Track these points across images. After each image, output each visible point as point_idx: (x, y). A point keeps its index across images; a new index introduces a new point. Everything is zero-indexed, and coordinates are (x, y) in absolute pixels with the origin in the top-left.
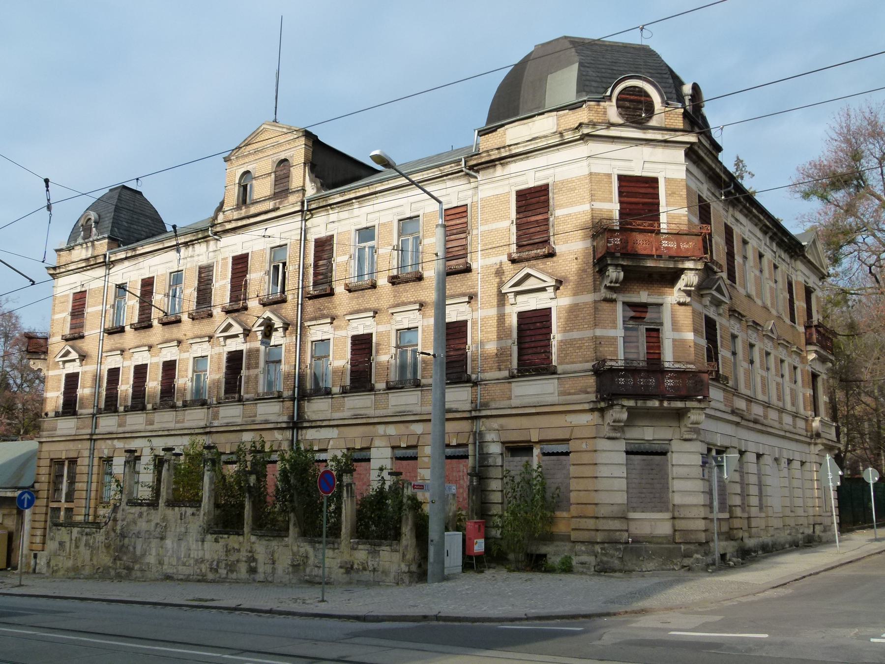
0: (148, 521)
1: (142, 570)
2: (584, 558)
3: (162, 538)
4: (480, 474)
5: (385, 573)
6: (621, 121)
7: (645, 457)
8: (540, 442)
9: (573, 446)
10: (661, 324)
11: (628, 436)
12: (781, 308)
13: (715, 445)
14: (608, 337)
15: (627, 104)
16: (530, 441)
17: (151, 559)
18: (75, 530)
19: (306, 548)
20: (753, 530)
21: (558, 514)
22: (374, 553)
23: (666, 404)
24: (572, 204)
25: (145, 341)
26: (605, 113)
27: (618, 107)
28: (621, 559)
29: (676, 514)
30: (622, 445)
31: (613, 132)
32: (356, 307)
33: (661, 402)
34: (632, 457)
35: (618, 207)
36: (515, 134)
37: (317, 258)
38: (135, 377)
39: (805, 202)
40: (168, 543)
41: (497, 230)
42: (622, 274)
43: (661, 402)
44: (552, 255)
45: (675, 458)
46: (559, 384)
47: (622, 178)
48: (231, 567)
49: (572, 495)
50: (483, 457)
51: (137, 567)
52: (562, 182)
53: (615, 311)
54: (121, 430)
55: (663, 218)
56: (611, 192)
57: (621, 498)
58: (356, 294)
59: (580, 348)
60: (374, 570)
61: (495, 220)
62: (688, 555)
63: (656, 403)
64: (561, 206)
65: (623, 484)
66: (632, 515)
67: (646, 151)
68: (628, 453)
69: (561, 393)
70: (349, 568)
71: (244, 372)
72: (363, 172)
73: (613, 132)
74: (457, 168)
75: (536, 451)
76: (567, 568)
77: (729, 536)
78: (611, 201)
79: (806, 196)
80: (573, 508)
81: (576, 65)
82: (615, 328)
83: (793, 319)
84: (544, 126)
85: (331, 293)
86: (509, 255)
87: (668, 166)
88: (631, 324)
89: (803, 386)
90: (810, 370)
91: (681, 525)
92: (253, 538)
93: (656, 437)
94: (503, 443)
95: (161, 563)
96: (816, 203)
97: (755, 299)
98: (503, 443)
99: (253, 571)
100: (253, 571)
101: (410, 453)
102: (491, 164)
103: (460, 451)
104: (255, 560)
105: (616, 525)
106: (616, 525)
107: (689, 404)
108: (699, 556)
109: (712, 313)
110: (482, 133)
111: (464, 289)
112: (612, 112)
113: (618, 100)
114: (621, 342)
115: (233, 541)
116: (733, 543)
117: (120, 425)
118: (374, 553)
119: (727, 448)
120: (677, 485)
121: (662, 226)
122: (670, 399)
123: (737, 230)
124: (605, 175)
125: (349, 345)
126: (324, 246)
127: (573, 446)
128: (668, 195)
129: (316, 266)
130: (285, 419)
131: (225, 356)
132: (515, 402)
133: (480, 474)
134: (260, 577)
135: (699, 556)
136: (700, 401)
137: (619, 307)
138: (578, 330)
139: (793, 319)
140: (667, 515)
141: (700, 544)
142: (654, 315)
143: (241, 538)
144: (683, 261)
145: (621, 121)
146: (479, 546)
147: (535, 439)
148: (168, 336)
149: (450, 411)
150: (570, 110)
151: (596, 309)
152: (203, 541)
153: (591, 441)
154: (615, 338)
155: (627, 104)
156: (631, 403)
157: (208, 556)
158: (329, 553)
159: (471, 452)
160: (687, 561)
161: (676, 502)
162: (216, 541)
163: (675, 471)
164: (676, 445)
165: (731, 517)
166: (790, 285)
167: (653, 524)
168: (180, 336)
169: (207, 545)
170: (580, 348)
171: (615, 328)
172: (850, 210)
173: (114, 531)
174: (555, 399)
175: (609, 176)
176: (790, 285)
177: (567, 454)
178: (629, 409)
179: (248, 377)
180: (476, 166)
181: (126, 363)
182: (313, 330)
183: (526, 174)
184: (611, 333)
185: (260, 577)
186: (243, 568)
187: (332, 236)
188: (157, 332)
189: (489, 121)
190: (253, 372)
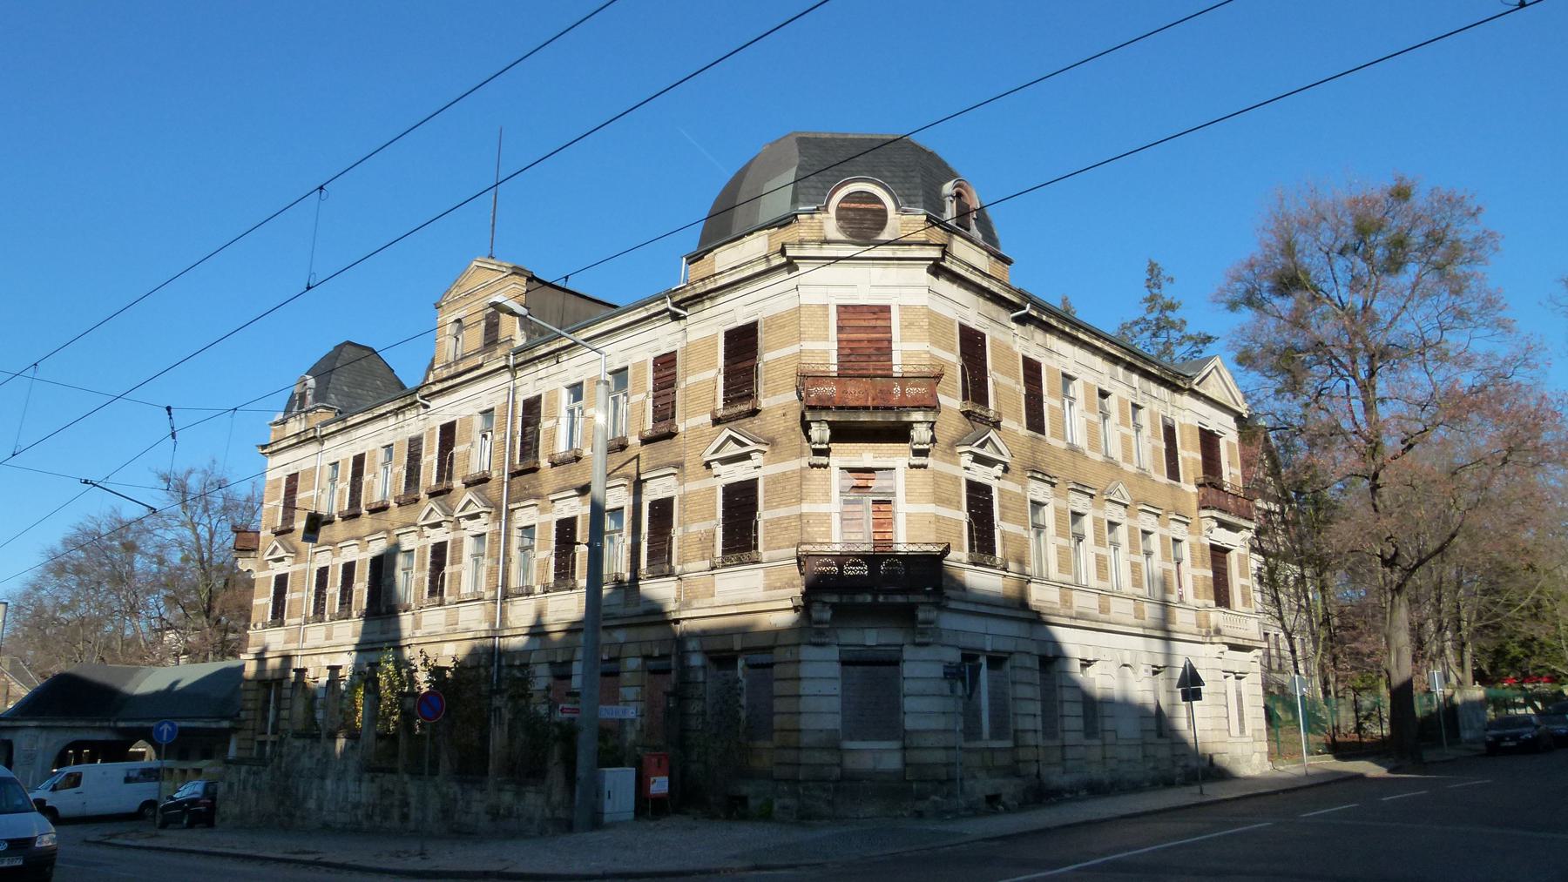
0: (311, 757)
1: (303, 818)
2: (788, 801)
3: (323, 778)
4: (681, 693)
5: (530, 820)
6: (842, 237)
7: (867, 668)
8: (744, 650)
9: (780, 655)
10: (893, 494)
11: (843, 641)
12: (1147, 463)
13: (984, 651)
14: (819, 514)
15: (851, 214)
16: (731, 650)
17: (312, 804)
18: (244, 769)
19: (454, 789)
20: (1069, 764)
21: (759, 744)
22: (519, 795)
23: (881, 599)
24: (783, 345)
25: (354, 533)
26: (821, 228)
27: (838, 219)
28: (830, 803)
29: (907, 742)
30: (833, 653)
31: (829, 251)
32: (563, 484)
33: (875, 596)
34: (851, 668)
35: (833, 346)
36: (726, 258)
37: (525, 424)
38: (344, 578)
39: (1234, 315)
40: (329, 783)
41: (703, 382)
42: (828, 433)
43: (875, 596)
44: (754, 412)
45: (907, 669)
46: (766, 575)
47: (843, 309)
48: (386, 815)
49: (777, 719)
50: (685, 669)
51: (298, 814)
52: (772, 318)
53: (828, 480)
54: (328, 643)
55: (896, 358)
56: (827, 328)
57: (833, 722)
58: (562, 468)
59: (786, 529)
60: (519, 817)
61: (703, 369)
62: (921, 797)
63: (869, 598)
64: (769, 349)
65: (836, 704)
66: (848, 745)
67: (876, 272)
68: (844, 663)
69: (769, 587)
70: (494, 814)
71: (447, 569)
72: (605, 311)
73: (829, 251)
74: (662, 307)
75: (741, 663)
76: (766, 816)
77: (1013, 771)
78: (826, 339)
79: (1233, 306)
80: (776, 736)
81: (794, 169)
82: (829, 501)
83: (1173, 473)
84: (755, 247)
85: (535, 470)
86: (713, 413)
87: (904, 290)
88: (853, 496)
89: (1193, 566)
90: (1207, 542)
91: (916, 756)
92: (406, 777)
93: (883, 641)
94: (706, 652)
95: (320, 808)
96: (1247, 315)
97: (1088, 453)
98: (706, 652)
99: (405, 817)
100: (405, 817)
101: (612, 666)
102: (698, 298)
103: (661, 664)
104: (407, 804)
105: (826, 757)
106: (826, 757)
107: (913, 598)
108: (937, 798)
109: (981, 474)
110: (694, 258)
111: (671, 458)
112: (829, 224)
113: (839, 209)
114: (836, 521)
115: (388, 781)
116: (1017, 781)
117: (328, 637)
118: (519, 795)
119: (1011, 653)
120: (909, 704)
121: (895, 369)
122: (888, 593)
123: (1046, 363)
124: (819, 306)
125: (554, 533)
126: (532, 408)
127: (780, 655)
128: (903, 327)
129: (524, 435)
130: (485, 626)
131: (429, 550)
132: (717, 600)
133: (681, 693)
134: (411, 825)
135: (937, 798)
136: (928, 594)
137: (835, 474)
138: (787, 505)
139: (1173, 473)
140: (895, 745)
141: (941, 782)
142: (885, 483)
143: (395, 778)
144: (908, 413)
145: (842, 237)
146: (659, 785)
147: (737, 646)
148: (377, 525)
149: (607, 617)
150: (780, 227)
151: (802, 477)
152: (360, 781)
153: (794, 650)
154: (828, 515)
155: (851, 214)
156: (835, 599)
157: (364, 800)
158: (477, 796)
159: (673, 665)
160: (921, 805)
161: (1020, 727)
162: (372, 780)
163: (907, 686)
164: (908, 653)
165: (1016, 746)
166: (1170, 433)
167: (877, 756)
168: (388, 525)
169: (364, 785)
170: (786, 529)
171: (829, 501)
172: (1298, 321)
173: (279, 768)
174: (760, 594)
175: (826, 306)
176: (1170, 433)
177: (770, 665)
178: (833, 606)
179: (452, 574)
180: (685, 304)
181: (335, 561)
182: (518, 514)
183: (734, 311)
184: (822, 508)
185: (411, 825)
186: (396, 813)
187: (539, 397)
188: (366, 522)
189: (700, 245)
190: (456, 568)
